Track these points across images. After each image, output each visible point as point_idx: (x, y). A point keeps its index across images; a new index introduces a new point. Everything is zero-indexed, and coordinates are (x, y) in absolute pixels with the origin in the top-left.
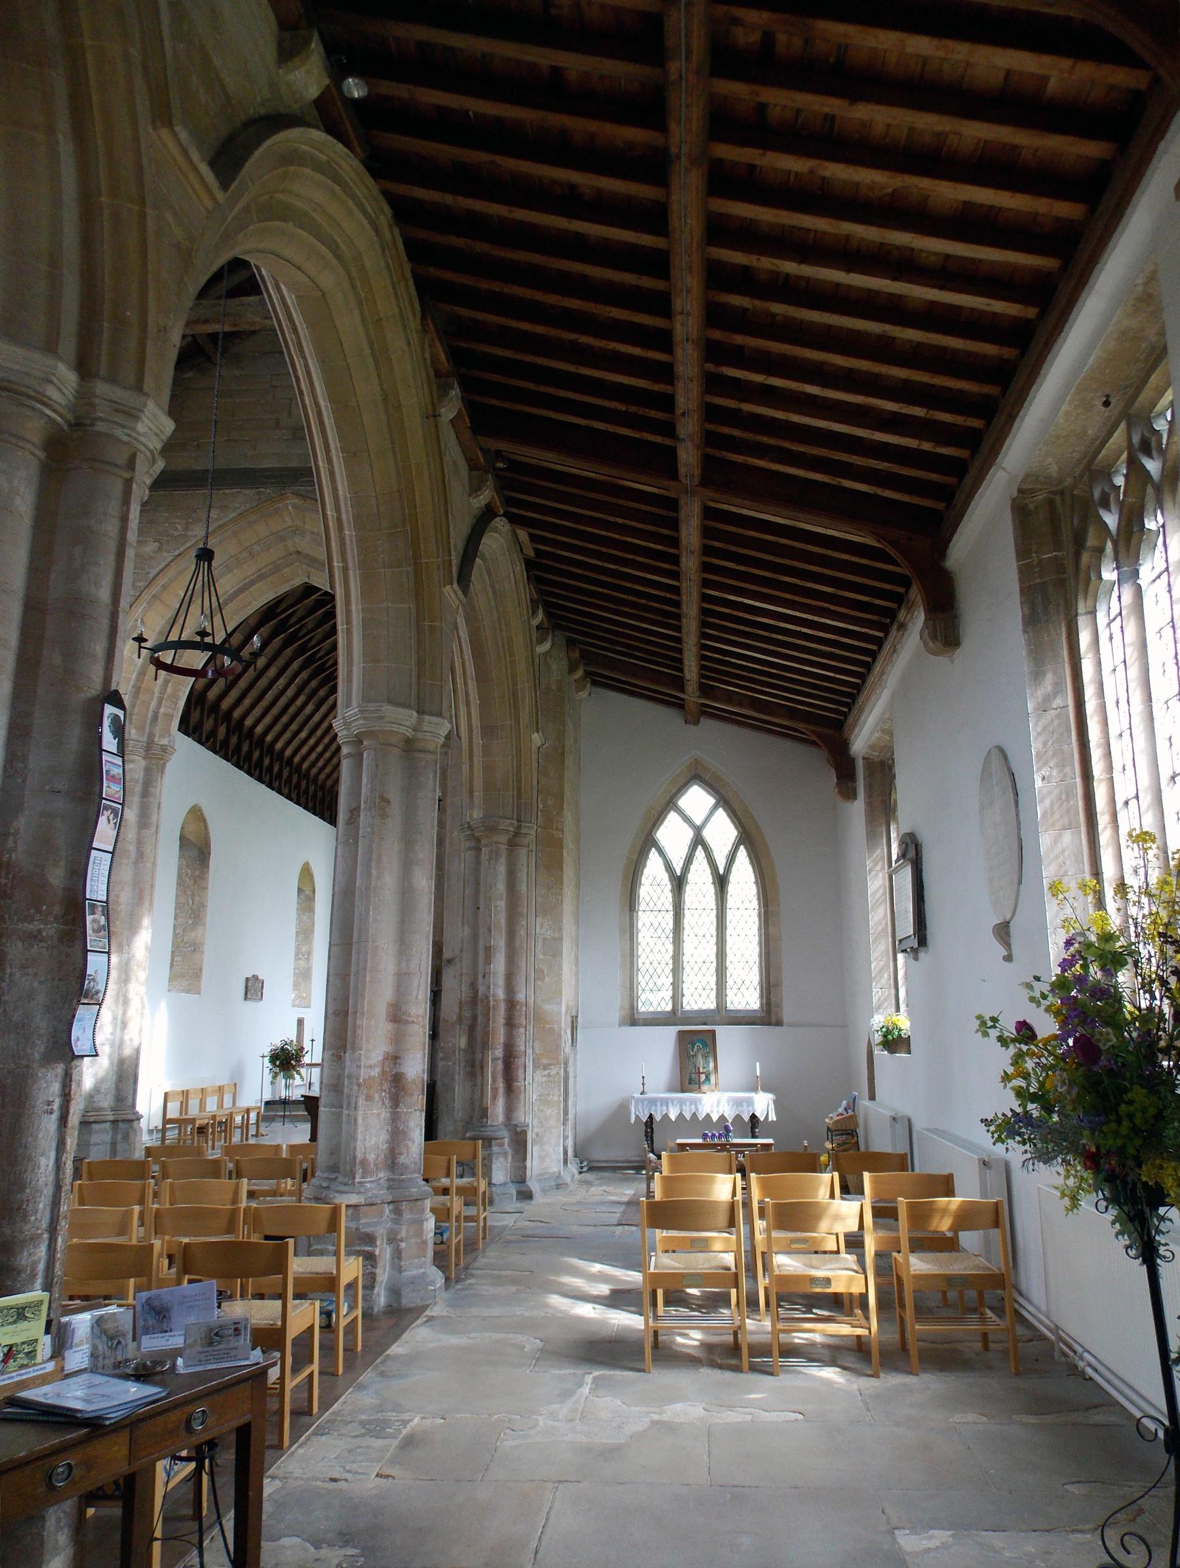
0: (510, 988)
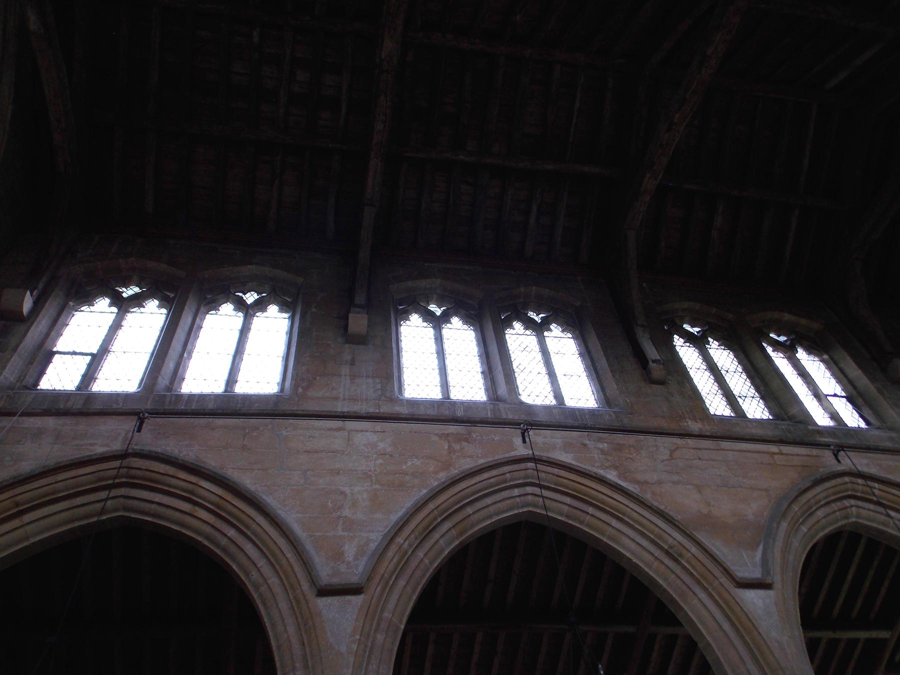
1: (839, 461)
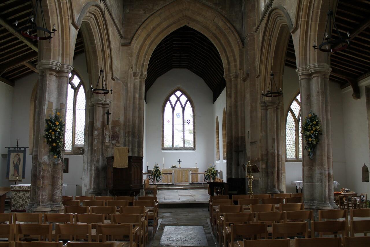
1: (100, 3)
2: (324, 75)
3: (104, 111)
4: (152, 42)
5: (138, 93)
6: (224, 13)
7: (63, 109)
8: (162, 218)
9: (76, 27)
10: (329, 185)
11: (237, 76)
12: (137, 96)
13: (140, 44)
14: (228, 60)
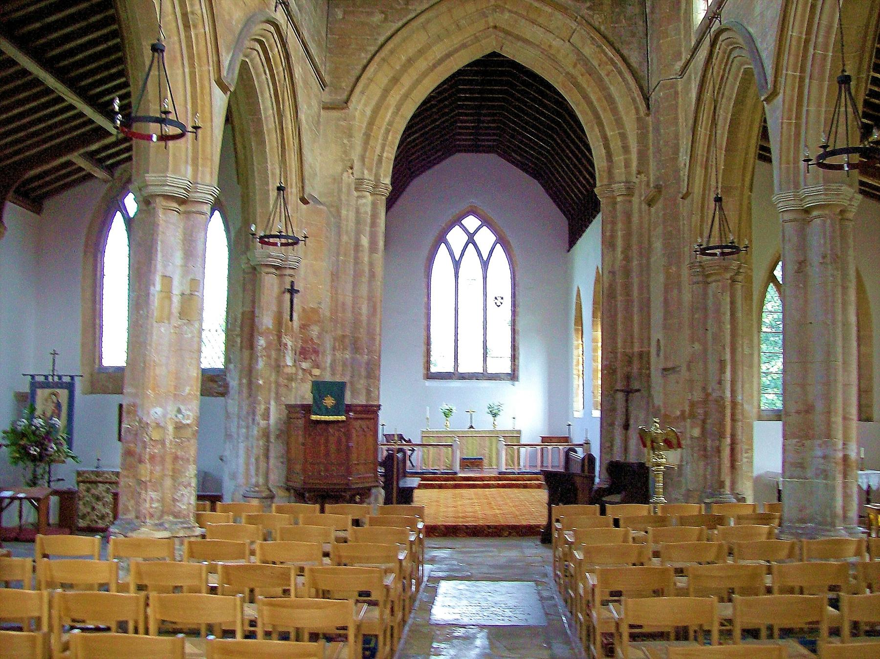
0: (733, 391)
1: (275, 10)
2: (842, 212)
3: (282, 283)
4: (406, 96)
5: (367, 235)
6: (597, 20)
7: (196, 293)
8: (432, 561)
9: (224, 88)
10: (845, 486)
11: (630, 191)
12: (365, 241)
13: (373, 103)
14: (607, 147)
